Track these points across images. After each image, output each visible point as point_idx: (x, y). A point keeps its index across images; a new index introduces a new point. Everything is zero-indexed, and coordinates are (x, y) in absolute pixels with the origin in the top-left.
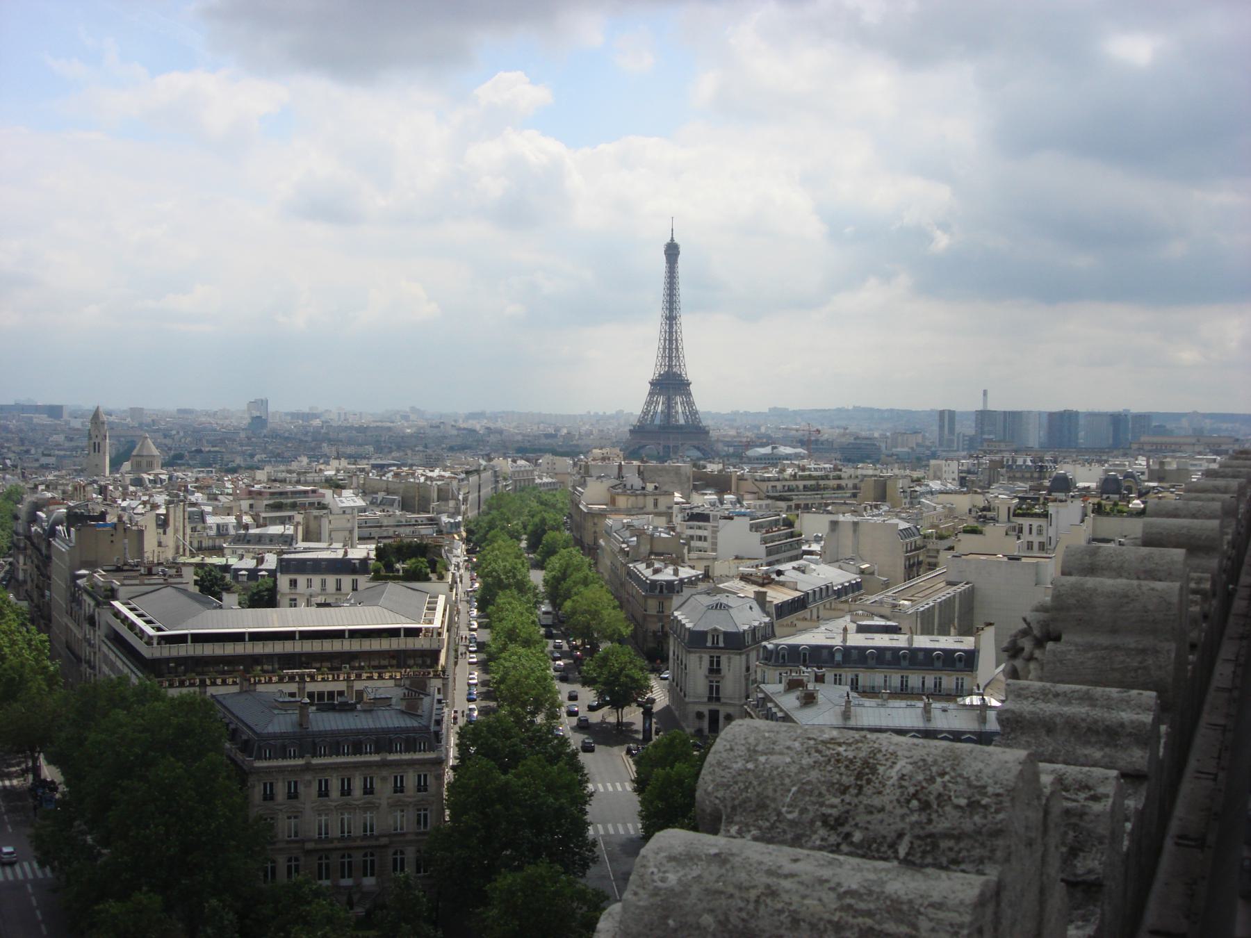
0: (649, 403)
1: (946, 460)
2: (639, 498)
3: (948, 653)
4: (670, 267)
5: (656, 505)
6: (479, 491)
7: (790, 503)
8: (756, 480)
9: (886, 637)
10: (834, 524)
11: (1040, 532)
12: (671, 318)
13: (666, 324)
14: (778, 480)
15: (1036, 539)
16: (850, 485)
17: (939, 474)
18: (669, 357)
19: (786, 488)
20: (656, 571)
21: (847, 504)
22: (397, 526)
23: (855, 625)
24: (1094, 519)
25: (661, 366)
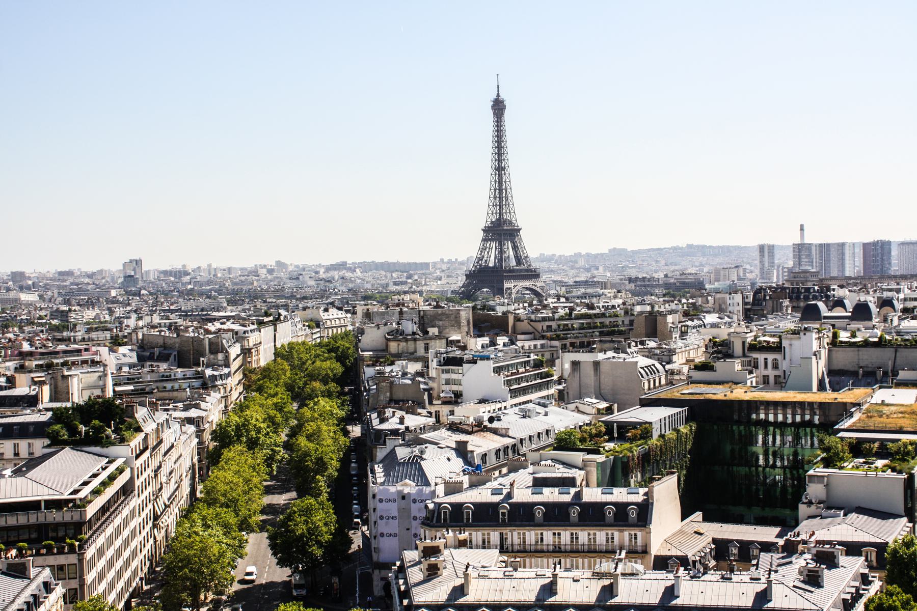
0: (483, 250)
1: (730, 294)
2: (409, 343)
3: (621, 508)
4: (497, 121)
5: (427, 349)
6: (275, 341)
7: (564, 342)
8: (532, 321)
9: (556, 490)
10: (575, 364)
11: (776, 366)
12: (500, 169)
13: (496, 174)
14: (553, 319)
15: (771, 372)
16: (627, 322)
17: (723, 306)
18: (500, 206)
19: (562, 327)
20: (383, 420)
21: (614, 341)
22: (162, 381)
23: (531, 476)
24: (829, 350)
25: (493, 213)
